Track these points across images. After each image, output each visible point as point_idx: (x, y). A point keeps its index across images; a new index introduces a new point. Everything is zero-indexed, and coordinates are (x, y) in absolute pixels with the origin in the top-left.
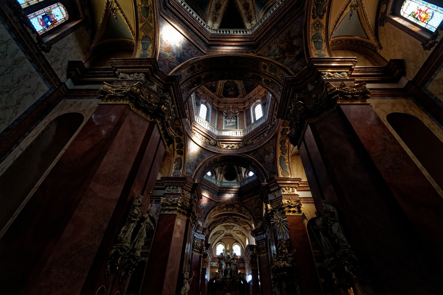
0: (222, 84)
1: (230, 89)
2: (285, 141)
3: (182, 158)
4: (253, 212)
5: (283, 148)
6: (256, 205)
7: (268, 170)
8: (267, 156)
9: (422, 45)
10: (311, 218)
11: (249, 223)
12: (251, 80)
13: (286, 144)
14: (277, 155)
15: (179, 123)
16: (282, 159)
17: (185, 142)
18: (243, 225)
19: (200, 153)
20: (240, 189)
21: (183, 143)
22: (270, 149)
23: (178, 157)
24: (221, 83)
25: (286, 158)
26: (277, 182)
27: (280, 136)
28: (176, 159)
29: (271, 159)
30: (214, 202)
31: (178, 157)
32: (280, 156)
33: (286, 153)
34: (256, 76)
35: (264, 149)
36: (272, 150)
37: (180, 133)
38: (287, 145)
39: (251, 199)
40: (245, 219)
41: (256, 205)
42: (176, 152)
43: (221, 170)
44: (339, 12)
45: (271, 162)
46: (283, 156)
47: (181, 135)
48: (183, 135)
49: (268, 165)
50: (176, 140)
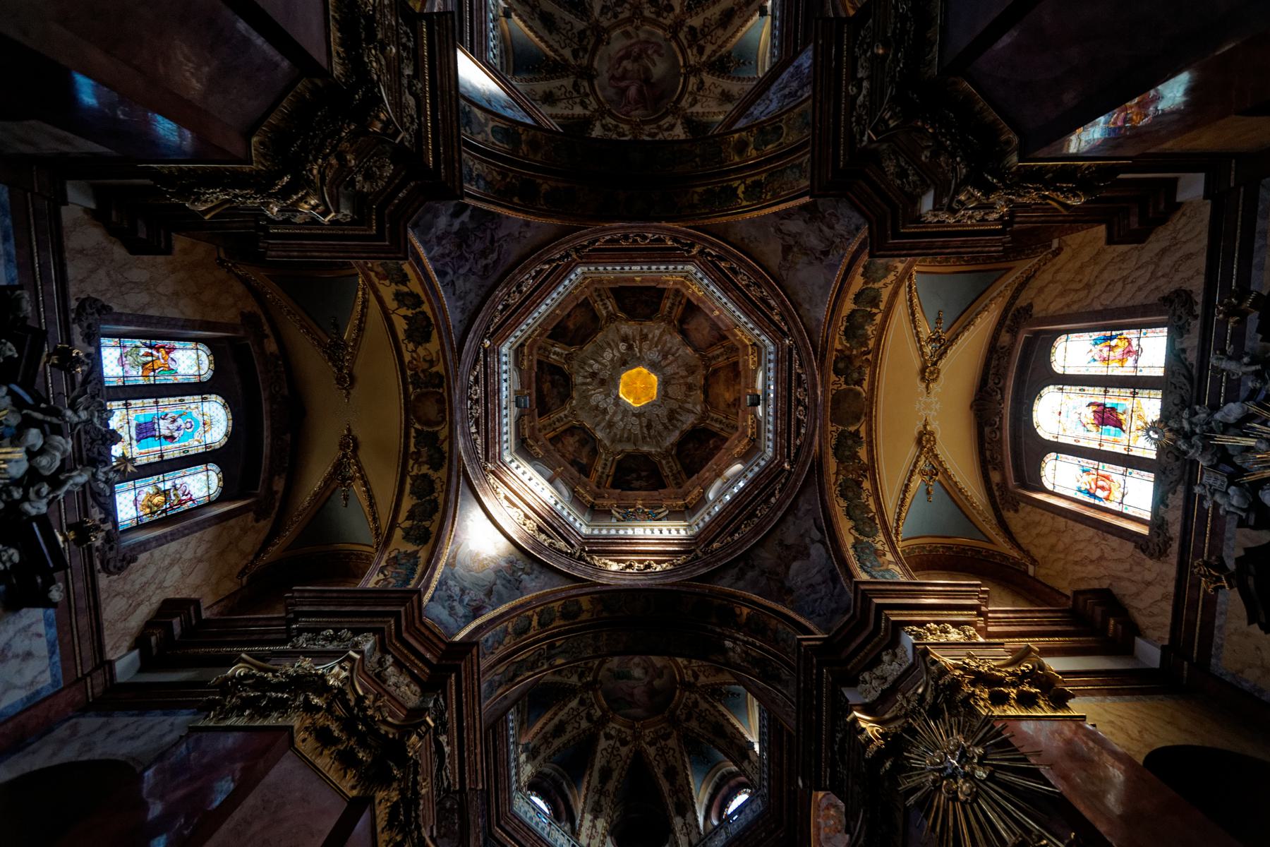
0: (609, 464)
1: (634, 475)
2: (859, 484)
3: (423, 555)
5: (858, 512)
7: (813, 612)
8: (795, 566)
9: (1136, 547)
12: (703, 211)
13: (864, 495)
14: (836, 527)
16: (867, 551)
17: (446, 501)
19: (503, 564)
21: (441, 500)
22: (802, 536)
23: (402, 550)
24: (606, 460)
25: (879, 546)
26: (870, 601)
28: (395, 557)
29: (816, 570)
31: (402, 550)
32: (853, 540)
33: (877, 530)
34: (717, 189)
35: (781, 543)
36: (816, 534)
37: (437, 456)
42: (398, 533)
43: (596, 797)
44: (898, 486)
46: (865, 539)
47: (436, 466)
48: (446, 466)
49: (808, 595)
50: (412, 485)
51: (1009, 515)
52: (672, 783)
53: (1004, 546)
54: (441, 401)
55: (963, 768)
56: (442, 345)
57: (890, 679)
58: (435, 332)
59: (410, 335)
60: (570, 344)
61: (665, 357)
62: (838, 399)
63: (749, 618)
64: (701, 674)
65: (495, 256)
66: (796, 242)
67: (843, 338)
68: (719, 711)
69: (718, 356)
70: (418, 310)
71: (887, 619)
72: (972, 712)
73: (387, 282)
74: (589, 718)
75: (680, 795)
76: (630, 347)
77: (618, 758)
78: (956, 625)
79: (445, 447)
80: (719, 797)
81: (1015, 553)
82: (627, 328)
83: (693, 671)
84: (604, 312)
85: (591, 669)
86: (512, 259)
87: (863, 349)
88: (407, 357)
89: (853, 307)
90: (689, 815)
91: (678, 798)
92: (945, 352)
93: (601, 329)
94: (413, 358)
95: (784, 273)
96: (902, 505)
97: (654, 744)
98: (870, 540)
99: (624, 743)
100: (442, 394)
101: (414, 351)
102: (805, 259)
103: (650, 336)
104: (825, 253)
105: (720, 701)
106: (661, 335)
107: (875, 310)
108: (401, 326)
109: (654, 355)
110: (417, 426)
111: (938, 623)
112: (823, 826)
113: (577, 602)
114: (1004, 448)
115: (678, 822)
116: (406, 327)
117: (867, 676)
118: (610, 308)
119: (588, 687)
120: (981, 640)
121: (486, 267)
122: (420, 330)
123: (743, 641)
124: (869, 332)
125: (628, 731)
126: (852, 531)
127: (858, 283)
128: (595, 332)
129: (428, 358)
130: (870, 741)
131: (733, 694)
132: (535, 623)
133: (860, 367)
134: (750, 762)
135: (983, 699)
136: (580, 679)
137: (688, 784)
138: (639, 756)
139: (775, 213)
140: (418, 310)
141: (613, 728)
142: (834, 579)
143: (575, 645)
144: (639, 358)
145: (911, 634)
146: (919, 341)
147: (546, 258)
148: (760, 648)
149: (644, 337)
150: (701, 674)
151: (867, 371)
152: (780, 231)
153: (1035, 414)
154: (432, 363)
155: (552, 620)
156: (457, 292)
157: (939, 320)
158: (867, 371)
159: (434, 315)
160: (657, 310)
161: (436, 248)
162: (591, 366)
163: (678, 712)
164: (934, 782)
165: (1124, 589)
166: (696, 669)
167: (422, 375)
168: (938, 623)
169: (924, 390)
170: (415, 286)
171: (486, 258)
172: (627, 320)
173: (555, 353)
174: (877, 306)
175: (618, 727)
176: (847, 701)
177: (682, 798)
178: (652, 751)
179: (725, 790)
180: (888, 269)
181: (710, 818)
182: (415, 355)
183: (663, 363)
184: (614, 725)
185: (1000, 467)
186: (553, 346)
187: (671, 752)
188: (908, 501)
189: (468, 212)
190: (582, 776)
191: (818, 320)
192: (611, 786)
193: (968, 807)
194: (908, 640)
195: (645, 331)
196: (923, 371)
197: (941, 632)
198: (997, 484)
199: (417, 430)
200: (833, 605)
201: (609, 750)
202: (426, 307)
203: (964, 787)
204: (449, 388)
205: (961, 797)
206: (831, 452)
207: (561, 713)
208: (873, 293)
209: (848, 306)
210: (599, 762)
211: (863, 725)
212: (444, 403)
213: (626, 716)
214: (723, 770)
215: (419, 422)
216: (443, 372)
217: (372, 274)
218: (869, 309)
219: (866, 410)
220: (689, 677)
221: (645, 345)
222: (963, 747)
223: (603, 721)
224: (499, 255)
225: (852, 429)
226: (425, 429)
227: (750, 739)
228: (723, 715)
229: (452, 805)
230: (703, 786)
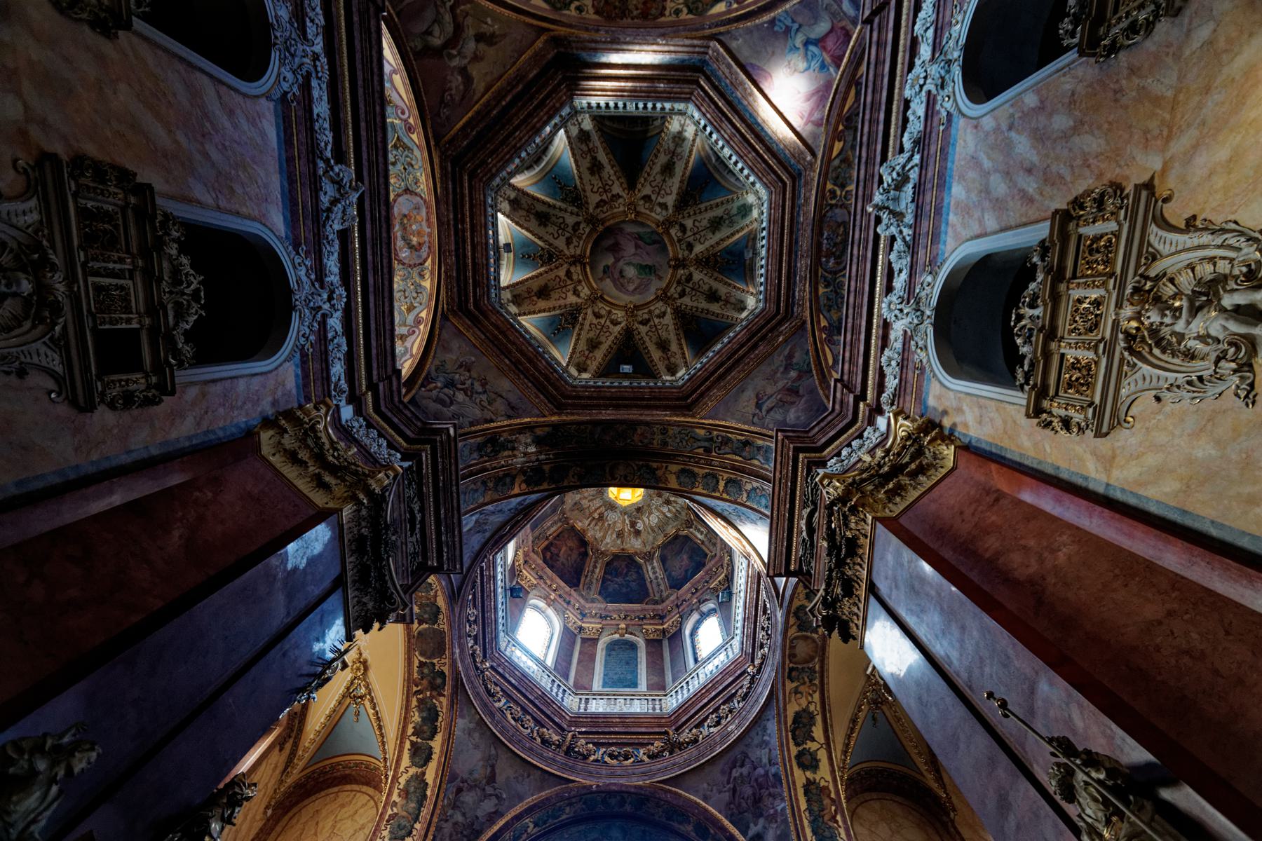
6: (456, 62)
15: (794, 647)
27: (441, 602)
30: (734, 45)
41: (456, 62)
52: (594, 158)
54: (792, 656)
56: (785, 710)
58: (790, 723)
59: (812, 717)
60: (686, 537)
61: (601, 516)
62: (440, 650)
64: (563, 278)
65: (735, 773)
66: (484, 789)
67: (439, 709)
69: (552, 526)
70: (801, 748)
73: (823, 783)
74: (683, 229)
75: (584, 148)
76: (633, 524)
77: (653, 184)
79: (792, 621)
82: (635, 545)
83: (572, 280)
84: (655, 564)
85: (679, 282)
86: (721, 764)
87: (421, 696)
88: (817, 696)
89: (432, 744)
91: (587, 145)
92: (348, 689)
93: (659, 547)
94: (811, 695)
95: (493, 752)
97: (613, 196)
99: (647, 198)
100: (791, 662)
101: (809, 703)
102: (476, 776)
103: (614, 536)
104: (459, 790)
105: (543, 249)
106: (604, 537)
107: (414, 738)
108: (818, 732)
109: (612, 517)
110: (815, 636)
112: (424, 223)
113: (680, 484)
116: (814, 729)
118: (649, 568)
119: (680, 263)
121: (742, 766)
122: (801, 725)
124: (417, 714)
125: (643, 210)
127: (430, 777)
128: (664, 546)
129: (799, 695)
132: (722, 484)
133: (422, 679)
136: (691, 275)
137: (576, 161)
138: (632, 185)
139: (502, 815)
140: (801, 748)
141: (659, 215)
143: (684, 443)
144: (625, 514)
146: (372, 700)
147: (692, 751)
149: (620, 534)
150: (563, 277)
151: (416, 675)
152: (497, 796)
154: (796, 691)
155: (705, 476)
156: (767, 750)
157: (357, 714)
158: (416, 675)
159: (787, 736)
160: (608, 564)
161: (779, 808)
162: (669, 511)
163: (587, 230)
166: (569, 282)
167: (806, 679)
169: (363, 651)
170: (800, 777)
171: (741, 774)
172: (636, 553)
173: (702, 533)
174: (413, 744)
175: (653, 214)
178: (617, 189)
180: (405, 793)
182: (810, 698)
183: (603, 509)
184: (658, 217)
186: (703, 543)
187: (595, 189)
189: (751, 833)
190: (690, 177)
191: (462, 717)
192: (663, 159)
195: (619, 542)
196: (366, 669)
199: (817, 633)
201: (663, 192)
202: (794, 750)
204: (784, 668)
206: (443, 609)
207: (712, 242)
208: (417, 760)
209: (437, 744)
210: (675, 184)
212: (789, 656)
213: (642, 224)
214: (537, 169)
215: (814, 641)
216: (788, 682)
217: (833, 795)
218: (419, 740)
219: (413, 641)
220: (576, 270)
221: (619, 526)
223: (668, 224)
224: (730, 773)
225: (425, 626)
226: (809, 634)
229: (828, 262)
230: (558, 154)
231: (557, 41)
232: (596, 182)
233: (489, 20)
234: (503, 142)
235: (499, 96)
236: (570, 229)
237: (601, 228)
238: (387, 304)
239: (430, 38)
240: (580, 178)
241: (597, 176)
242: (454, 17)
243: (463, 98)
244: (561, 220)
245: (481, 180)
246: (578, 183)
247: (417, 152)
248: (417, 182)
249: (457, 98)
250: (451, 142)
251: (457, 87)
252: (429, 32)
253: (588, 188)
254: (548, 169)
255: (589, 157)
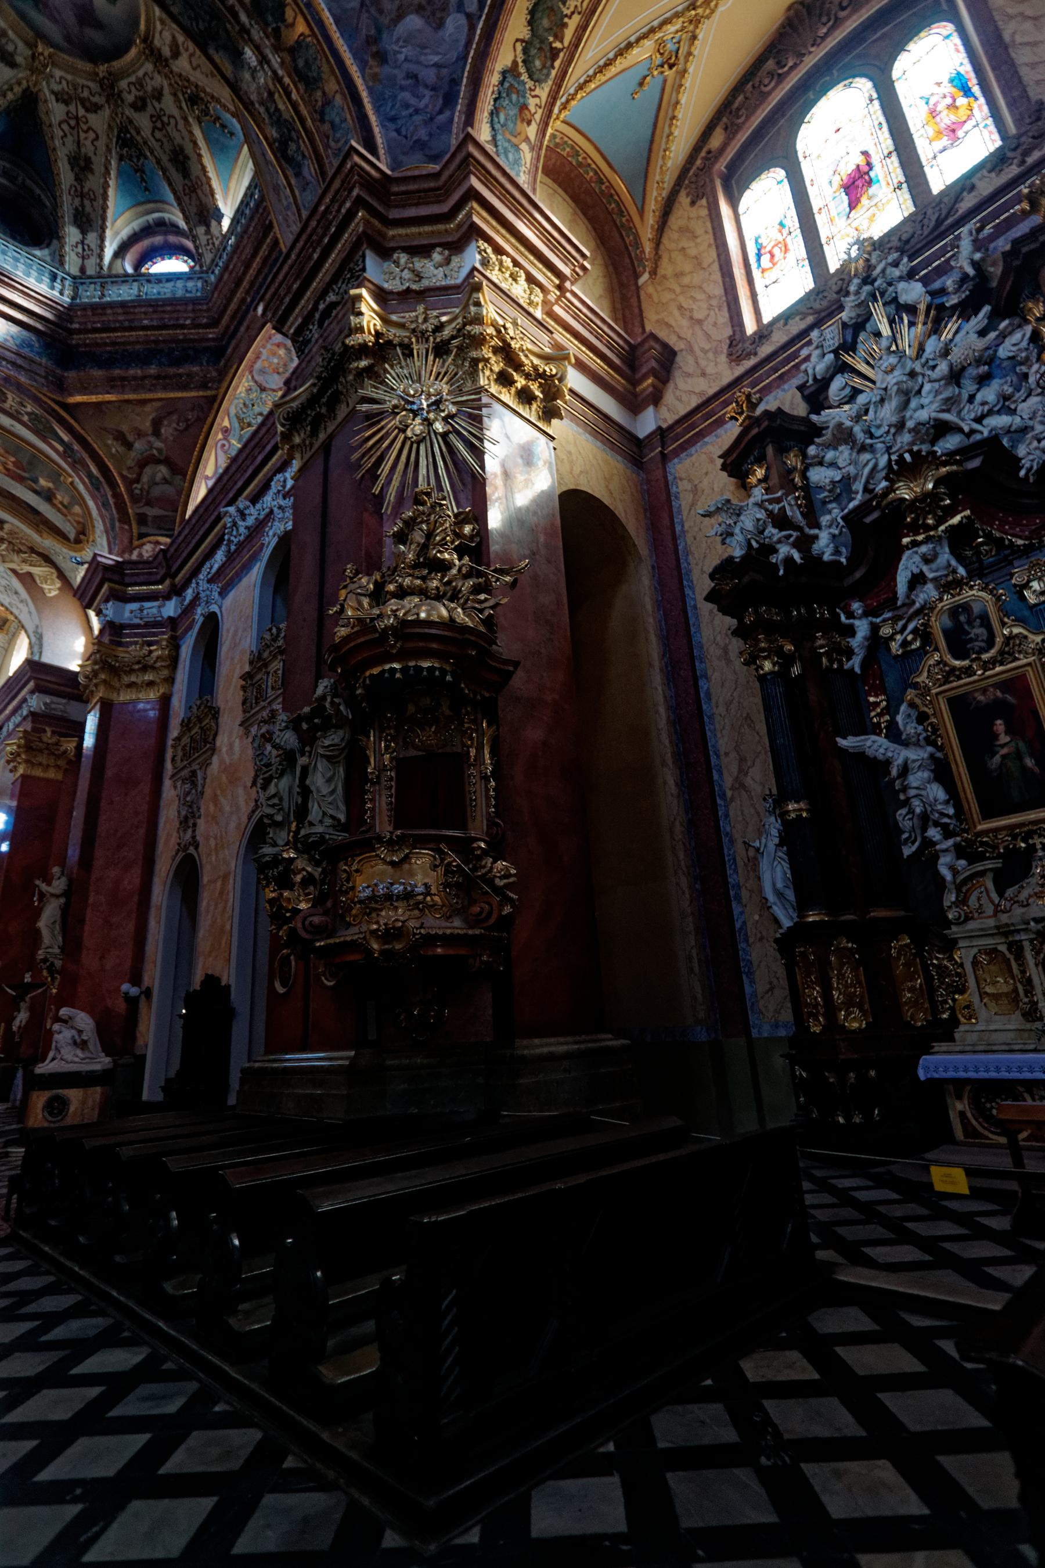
4: (123, 477)
6: (158, 444)
7: (393, 119)
8: (413, 22)
10: (572, 487)
11: (59, 560)
16: (514, 97)
18: (15, 557)
20: (65, 316)
25: (532, 103)
26: (466, 177)
29: (436, 59)
38: (576, 18)
39: (128, 401)
40: (39, 532)
45: (429, 75)
46: (525, 77)
51: (684, 199)
53: (646, 232)
55: (428, 413)
57: (425, 283)
63: (300, 44)
68: (191, 133)
71: (469, 215)
72: (474, 374)
75: (87, 202)
78: (531, 279)
80: (146, 243)
81: (648, 248)
90: (92, 238)
96: (600, 70)
97: (66, 103)
98: (530, 84)
111: (516, 263)
112: (264, 357)
114: (759, 111)
115: (72, 234)
117: (403, 258)
120: (538, 314)
123: (275, 72)
126: (519, 47)
130: (360, 329)
131: (223, 126)
134: (208, 232)
135: (491, 370)
142: (449, 100)
145: (480, 253)
148: (295, 106)
153: (814, 110)
164: (395, 407)
165: (685, 362)
168: (516, 263)
176: (364, 270)
177: (88, 209)
178: (57, 111)
179: (158, 240)
181: (123, 259)
185: (732, 131)
188: (613, 70)
193: (408, 443)
194: (472, 256)
197: (511, 275)
198: (709, 152)
200: (422, 134)
203: (417, 427)
205: (409, 433)
211: (364, 308)
222: (441, 398)
227: (221, 204)
228: (195, 144)
230: (127, 215)
231: (60, 386)
232: (88, 149)
233: (114, 450)
234: (165, 327)
235: (139, 384)
236: (150, 110)
237: (102, 69)
238: (260, 435)
239: (167, 476)
240: (107, 172)
241: (83, 150)
242: (140, 475)
243: (170, 413)
244: (158, 135)
245: (208, 310)
246: (114, 163)
247: (233, 411)
248: (249, 390)
249: (175, 417)
250: (204, 386)
251: (169, 425)
252: (165, 481)
253: (101, 144)
254: (152, 205)
255: (87, 185)
